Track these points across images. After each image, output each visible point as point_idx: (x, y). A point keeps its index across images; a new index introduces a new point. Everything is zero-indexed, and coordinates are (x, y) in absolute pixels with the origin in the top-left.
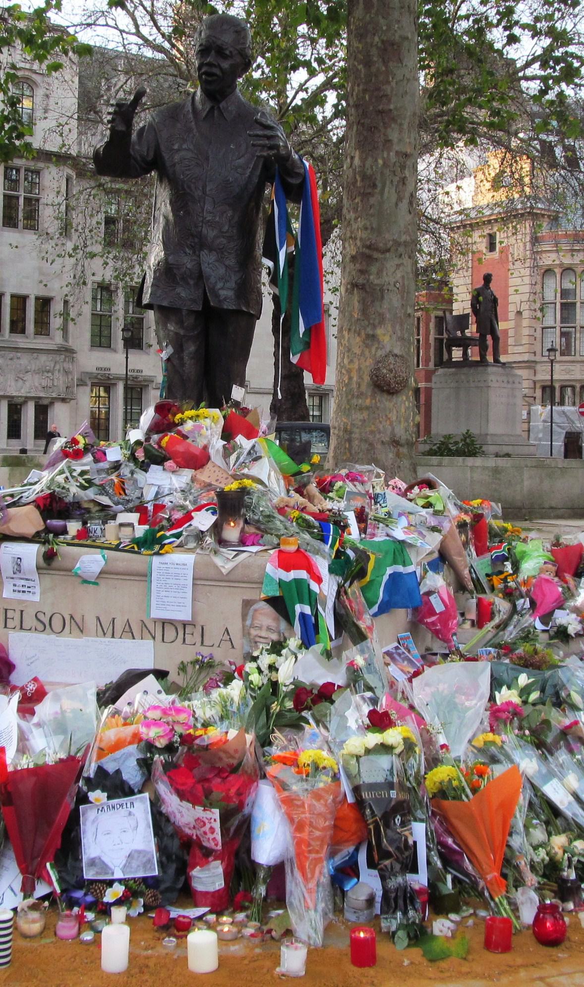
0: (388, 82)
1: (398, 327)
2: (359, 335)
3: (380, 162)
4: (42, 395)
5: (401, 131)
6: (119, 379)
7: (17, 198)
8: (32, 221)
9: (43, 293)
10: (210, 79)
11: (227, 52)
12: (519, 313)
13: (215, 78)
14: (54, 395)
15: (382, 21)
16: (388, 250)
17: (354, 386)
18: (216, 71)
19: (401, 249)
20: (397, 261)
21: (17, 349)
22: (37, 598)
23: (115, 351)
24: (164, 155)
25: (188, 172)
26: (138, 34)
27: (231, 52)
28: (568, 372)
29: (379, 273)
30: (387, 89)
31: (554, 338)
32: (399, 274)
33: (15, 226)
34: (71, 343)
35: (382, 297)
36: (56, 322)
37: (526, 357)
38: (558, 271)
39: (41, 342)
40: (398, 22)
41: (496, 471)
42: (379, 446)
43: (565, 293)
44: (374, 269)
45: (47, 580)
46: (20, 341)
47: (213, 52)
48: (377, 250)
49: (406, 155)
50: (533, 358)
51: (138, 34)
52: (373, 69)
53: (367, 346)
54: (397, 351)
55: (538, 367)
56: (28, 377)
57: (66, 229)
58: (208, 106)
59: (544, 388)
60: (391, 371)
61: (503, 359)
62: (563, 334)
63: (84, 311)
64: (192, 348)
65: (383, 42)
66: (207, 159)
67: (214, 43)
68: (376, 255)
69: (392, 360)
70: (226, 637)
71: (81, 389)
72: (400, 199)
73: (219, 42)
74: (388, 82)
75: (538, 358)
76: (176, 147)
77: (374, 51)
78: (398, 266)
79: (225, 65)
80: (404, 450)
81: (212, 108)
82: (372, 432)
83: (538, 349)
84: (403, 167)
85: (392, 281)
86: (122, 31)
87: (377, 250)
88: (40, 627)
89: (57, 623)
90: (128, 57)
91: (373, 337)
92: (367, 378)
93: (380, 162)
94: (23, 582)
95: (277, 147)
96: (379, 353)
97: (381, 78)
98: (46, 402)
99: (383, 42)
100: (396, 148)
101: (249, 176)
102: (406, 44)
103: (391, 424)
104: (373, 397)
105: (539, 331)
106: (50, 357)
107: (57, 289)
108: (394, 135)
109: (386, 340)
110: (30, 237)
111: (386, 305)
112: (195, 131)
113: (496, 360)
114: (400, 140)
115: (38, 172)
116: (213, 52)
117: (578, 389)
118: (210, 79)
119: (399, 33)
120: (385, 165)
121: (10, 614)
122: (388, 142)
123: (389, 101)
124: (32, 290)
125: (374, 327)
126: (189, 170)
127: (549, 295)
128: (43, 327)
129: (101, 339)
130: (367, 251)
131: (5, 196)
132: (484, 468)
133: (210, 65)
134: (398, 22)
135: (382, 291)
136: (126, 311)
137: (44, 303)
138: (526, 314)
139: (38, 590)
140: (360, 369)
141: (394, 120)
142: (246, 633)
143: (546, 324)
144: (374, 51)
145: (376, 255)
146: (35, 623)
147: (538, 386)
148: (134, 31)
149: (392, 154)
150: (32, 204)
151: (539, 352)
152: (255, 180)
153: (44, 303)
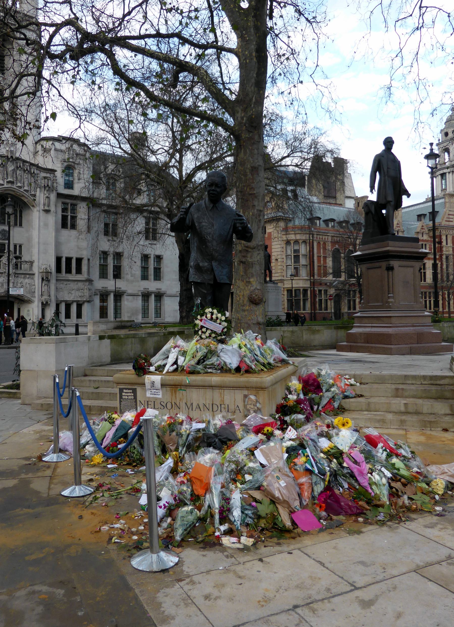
0: (253, 183)
1: (258, 278)
2: (243, 281)
3: (251, 213)
4: (79, 299)
5: (259, 202)
6: (111, 292)
7: (67, 216)
8: (73, 227)
9: (79, 256)
12: (277, 260)
14: (85, 299)
15: (251, 159)
16: (255, 248)
17: (241, 301)
19: (259, 248)
20: (258, 252)
21: (68, 280)
22: (160, 396)
23: (110, 280)
26: (120, 147)
28: (297, 284)
29: (251, 257)
30: (253, 185)
31: (291, 271)
32: (259, 257)
33: (67, 228)
34: (92, 277)
35: (253, 267)
36: (84, 268)
37: (280, 278)
38: (292, 242)
39: (79, 277)
40: (257, 159)
41: (292, 332)
42: (252, 325)
43: (295, 251)
44: (249, 255)
45: (164, 389)
46: (70, 277)
48: (250, 248)
49: (261, 211)
50: (283, 278)
51: (120, 147)
52: (248, 178)
53: (247, 286)
54: (258, 288)
55: (285, 282)
56: (73, 292)
57: (89, 229)
58: (212, 205)
59: (288, 291)
60: (256, 295)
61: (273, 279)
62: (295, 268)
63: (96, 263)
64: (210, 298)
65: (252, 167)
68: (250, 250)
69: (257, 291)
70: (238, 409)
71: (96, 296)
72: (259, 228)
74: (253, 183)
75: (285, 278)
77: (248, 171)
78: (258, 254)
79: (218, 190)
80: (262, 326)
82: (249, 320)
83: (284, 274)
84: (259, 216)
85: (256, 260)
86: (112, 146)
87: (250, 248)
88: (163, 408)
89: (169, 406)
90: (113, 156)
91: (249, 282)
92: (246, 299)
93: (251, 213)
94: (155, 391)
95: (244, 223)
96: (252, 288)
97: (251, 181)
98: (81, 303)
99: (252, 167)
100: (257, 208)
102: (260, 167)
103: (257, 316)
104: (249, 306)
105: (285, 267)
106: (82, 283)
107: (85, 254)
108: (256, 203)
109: (254, 283)
110: (73, 233)
111: (254, 270)
113: (271, 280)
114: (258, 205)
115: (76, 205)
117: (301, 291)
119: (258, 164)
120: (253, 215)
121: (150, 403)
122: (254, 206)
123: (254, 190)
124: (74, 255)
125: (249, 278)
127: (289, 252)
128: (79, 271)
129: (103, 275)
130: (246, 249)
131: (62, 215)
132: (288, 331)
133: (213, 190)
134: (257, 159)
135: (252, 264)
136: (114, 263)
137: (79, 261)
138: (279, 260)
139: (161, 393)
140: (243, 295)
141: (256, 197)
142: (245, 406)
143: (288, 264)
144: (248, 171)
145: (250, 250)
146: (160, 406)
147: (285, 289)
148: (118, 146)
149: (255, 210)
150: (74, 218)
151: (285, 275)
152: (231, 233)
153: (79, 261)
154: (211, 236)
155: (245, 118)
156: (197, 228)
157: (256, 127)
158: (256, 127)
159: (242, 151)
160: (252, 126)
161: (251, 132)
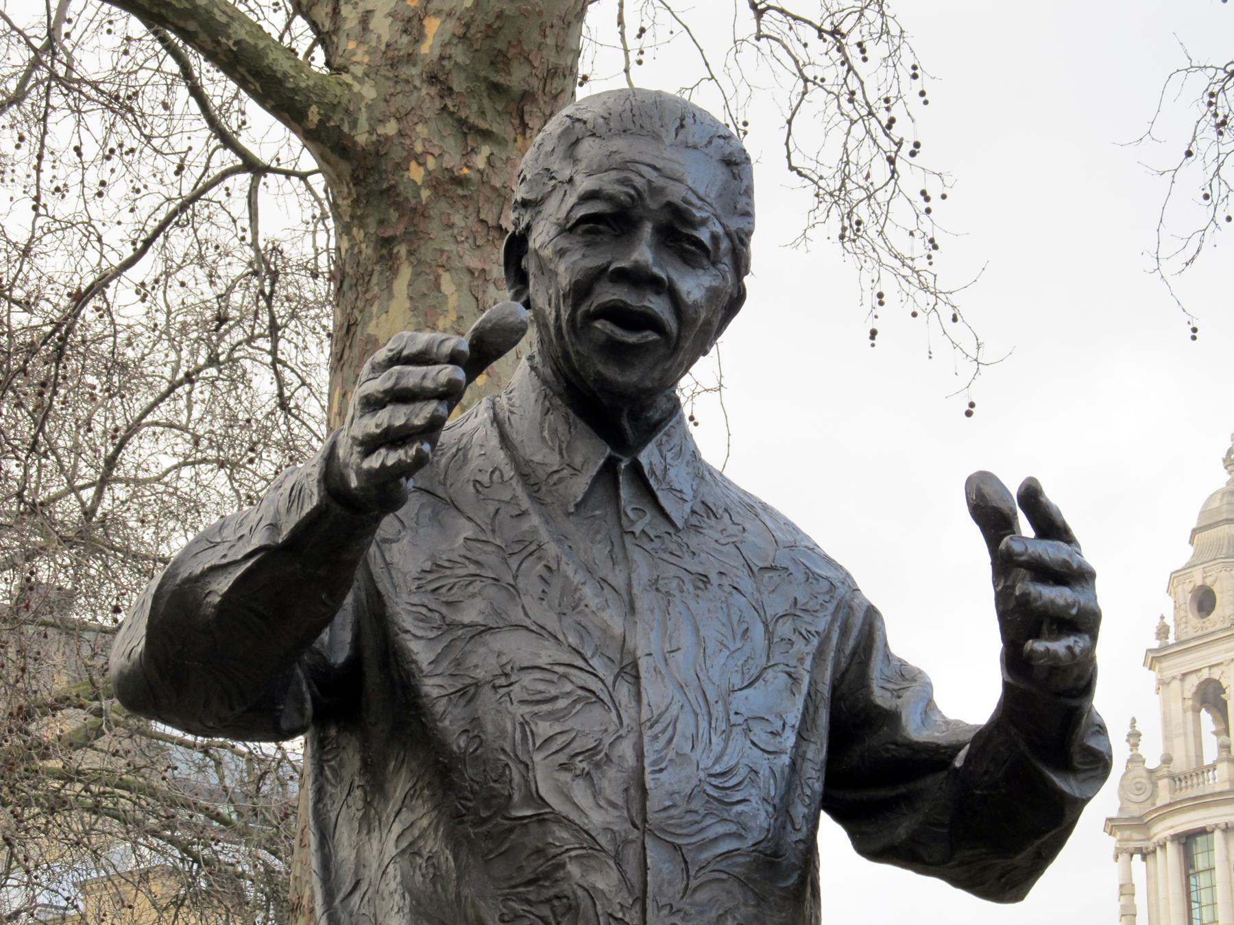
10: (632, 338)
11: (704, 235)
13: (652, 336)
18: (658, 305)
24: (414, 646)
25: (544, 729)
27: (715, 238)
47: (647, 229)
66: (630, 671)
67: (655, 191)
73: (676, 193)
76: (470, 614)
81: (610, 468)
101: (793, 763)
112: (552, 549)
116: (647, 229)
118: (632, 338)
126: (554, 716)
154: (612, 783)
155: (432, 26)
156: (431, 687)
157: (527, 96)
158: (527, 96)
159: (401, 284)
160: (496, 89)
161: (486, 135)
